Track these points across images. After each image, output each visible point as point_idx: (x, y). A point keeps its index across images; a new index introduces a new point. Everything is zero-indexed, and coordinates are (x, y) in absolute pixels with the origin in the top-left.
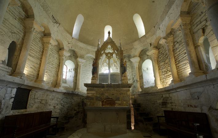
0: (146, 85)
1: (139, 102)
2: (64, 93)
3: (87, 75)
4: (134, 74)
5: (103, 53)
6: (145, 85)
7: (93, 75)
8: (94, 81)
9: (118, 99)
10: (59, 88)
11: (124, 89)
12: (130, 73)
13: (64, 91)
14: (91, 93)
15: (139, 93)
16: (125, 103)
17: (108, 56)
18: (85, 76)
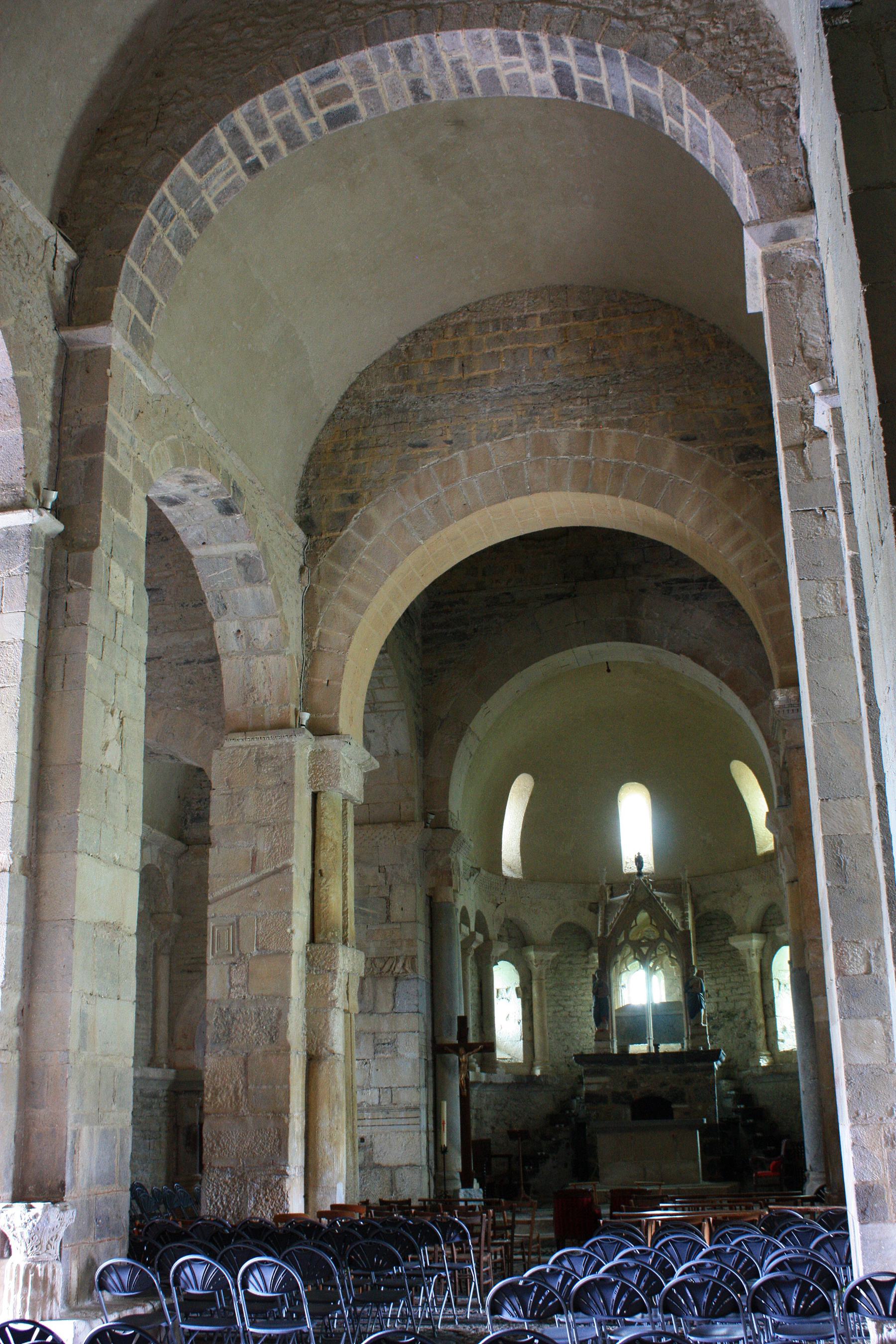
0: (786, 1041)
1: (761, 1103)
2: (508, 1086)
3: (564, 1003)
4: (747, 996)
5: (623, 944)
6: (783, 1041)
7: (597, 1024)
8: (603, 1044)
9: (679, 1097)
10: (495, 1072)
11: (697, 1065)
12: (732, 988)
13: (509, 1079)
14: (598, 1083)
15: (760, 1073)
16: (700, 1107)
17: (640, 952)
18: (557, 1009)
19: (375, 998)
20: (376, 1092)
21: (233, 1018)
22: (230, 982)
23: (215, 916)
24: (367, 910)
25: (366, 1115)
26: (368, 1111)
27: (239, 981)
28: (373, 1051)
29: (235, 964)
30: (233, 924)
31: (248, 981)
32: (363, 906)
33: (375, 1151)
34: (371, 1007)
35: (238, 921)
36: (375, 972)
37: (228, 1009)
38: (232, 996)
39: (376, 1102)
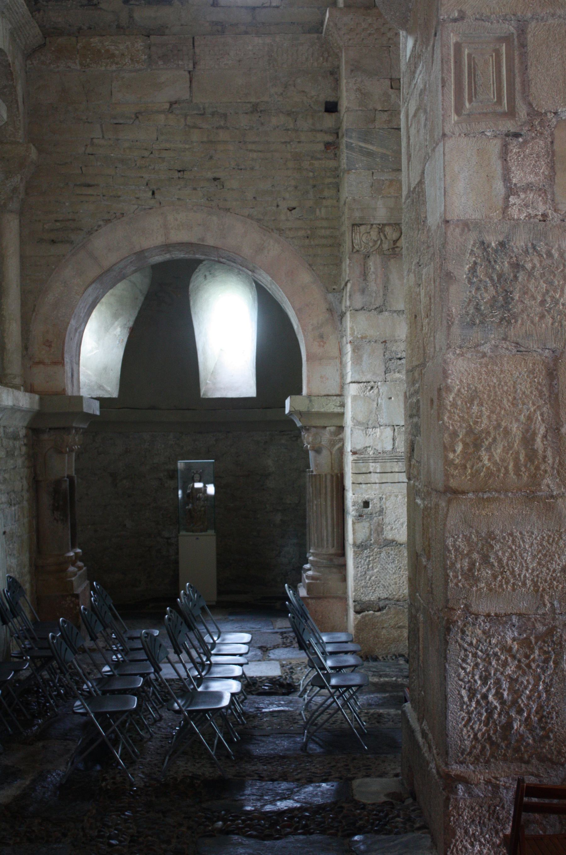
19: (385, 288)
20: (388, 432)
21: (517, 266)
22: (506, 179)
23: (462, 17)
24: (370, 147)
25: (372, 466)
26: (375, 460)
27: (531, 178)
28: (383, 368)
29: (517, 135)
30: (507, 39)
31: (551, 178)
32: (365, 141)
33: (387, 520)
34: (379, 302)
35: (522, 31)
36: (385, 246)
37: (502, 244)
38: (514, 212)
39: (389, 447)
